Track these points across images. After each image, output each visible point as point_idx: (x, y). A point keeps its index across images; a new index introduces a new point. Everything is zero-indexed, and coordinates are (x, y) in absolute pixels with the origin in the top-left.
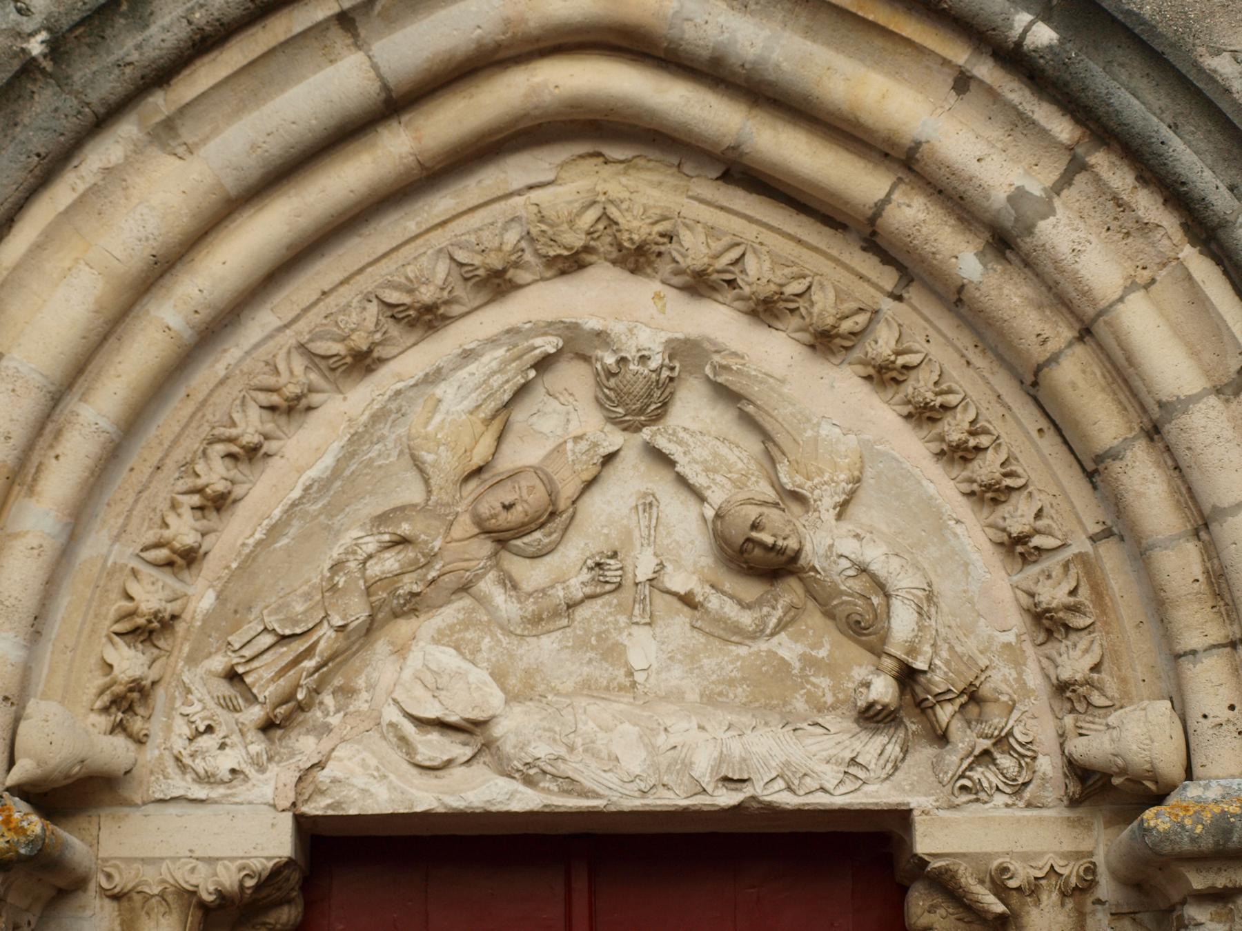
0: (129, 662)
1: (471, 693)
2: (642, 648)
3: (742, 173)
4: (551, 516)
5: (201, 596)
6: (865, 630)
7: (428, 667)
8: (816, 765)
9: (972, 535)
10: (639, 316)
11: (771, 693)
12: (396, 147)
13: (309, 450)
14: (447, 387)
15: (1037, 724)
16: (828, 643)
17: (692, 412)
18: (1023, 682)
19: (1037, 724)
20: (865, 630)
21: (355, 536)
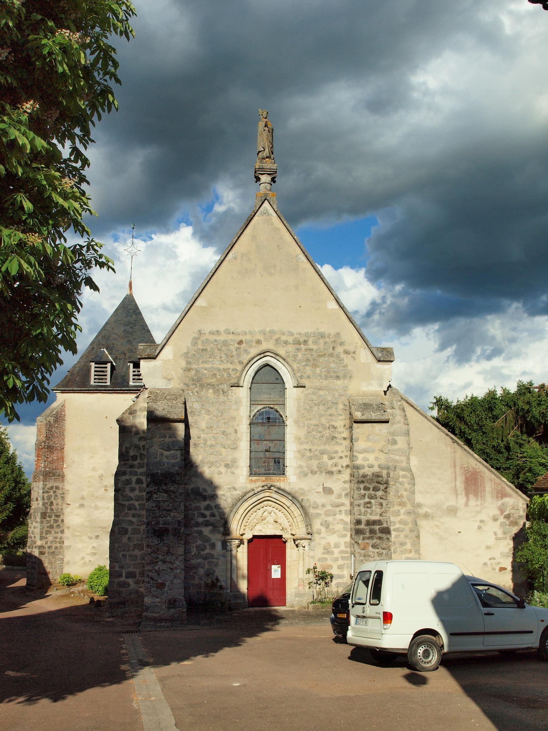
0: (244, 528)
1: (261, 528)
2: (270, 526)
3: (275, 503)
4: (265, 519)
5: (248, 524)
6: (281, 525)
7: (258, 527)
8: (278, 533)
9: (286, 521)
10: (270, 509)
11: (276, 528)
12: (258, 502)
13: (253, 516)
14: (260, 512)
15: (289, 530)
16: (279, 526)
17: (272, 513)
18: (289, 528)
19: (289, 530)
20: (281, 525)
21: (255, 520)
